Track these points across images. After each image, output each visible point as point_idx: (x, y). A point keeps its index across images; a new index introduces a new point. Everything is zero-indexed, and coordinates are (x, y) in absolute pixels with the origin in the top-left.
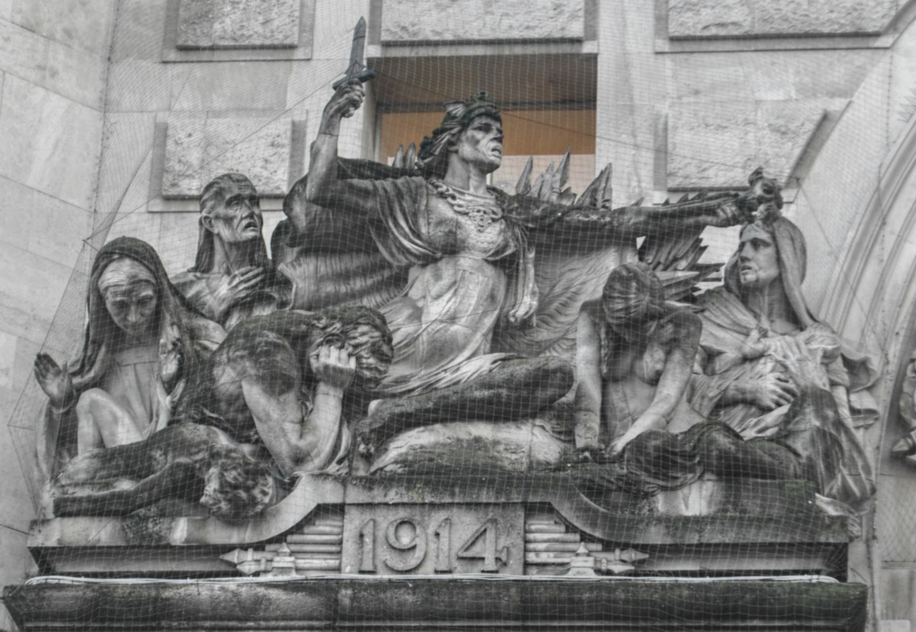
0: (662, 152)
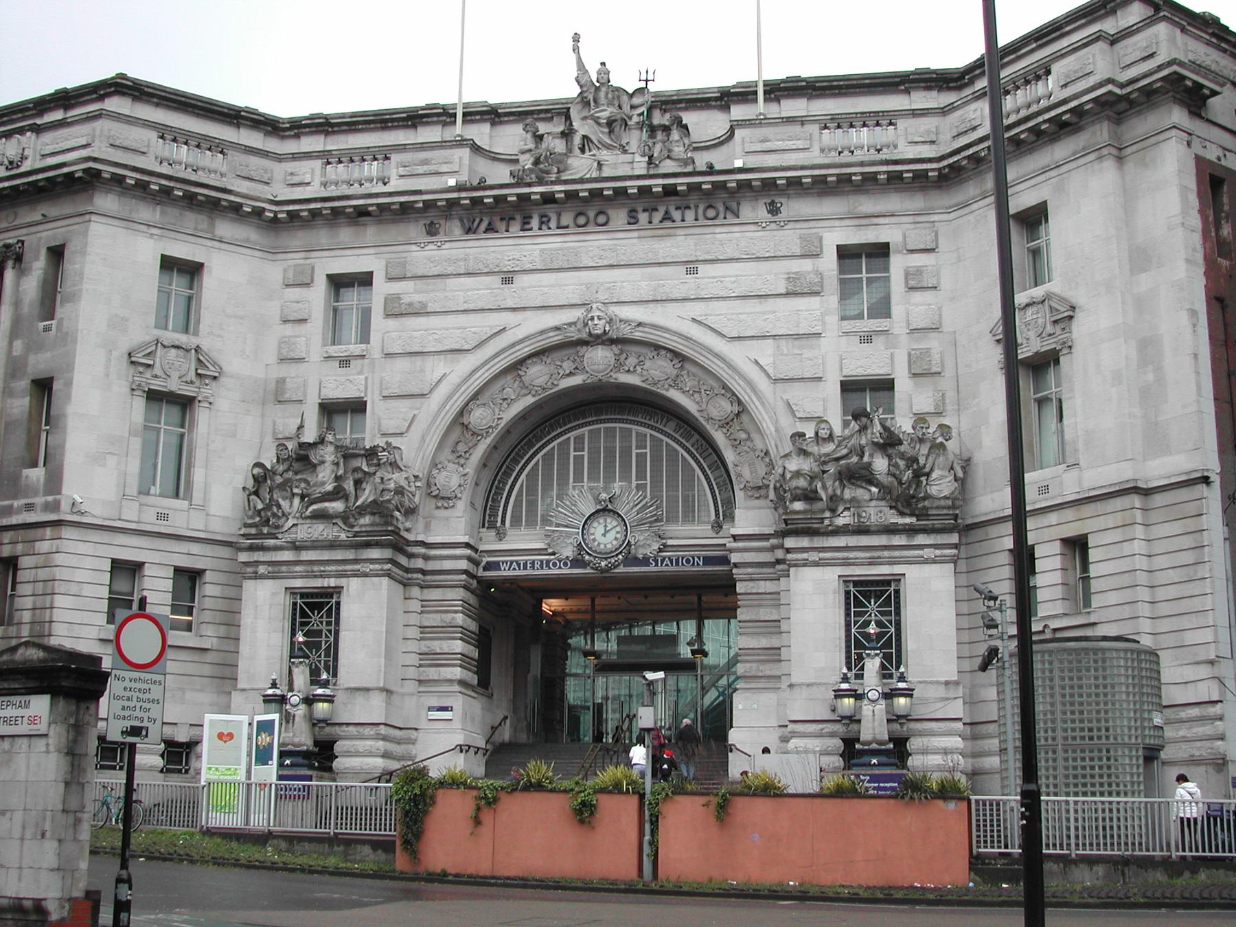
0: (379, 425)
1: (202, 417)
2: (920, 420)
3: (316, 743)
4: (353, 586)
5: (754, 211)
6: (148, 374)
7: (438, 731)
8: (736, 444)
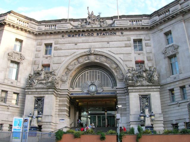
1: (21, 66)
2: (150, 67)
3: (38, 126)
4: (46, 96)
5: (118, 33)
6: (11, 57)
7: (61, 124)
8: (116, 72)
